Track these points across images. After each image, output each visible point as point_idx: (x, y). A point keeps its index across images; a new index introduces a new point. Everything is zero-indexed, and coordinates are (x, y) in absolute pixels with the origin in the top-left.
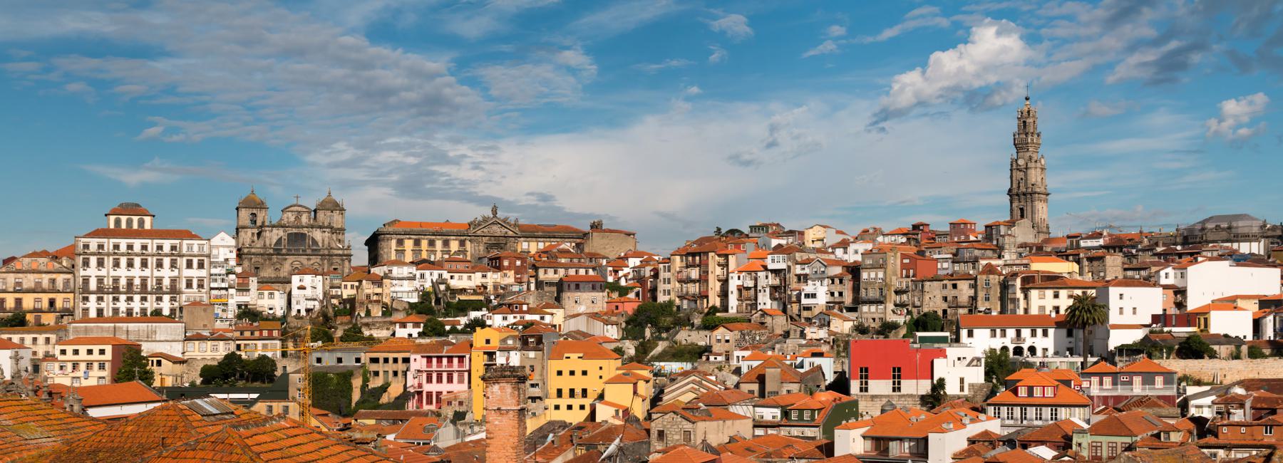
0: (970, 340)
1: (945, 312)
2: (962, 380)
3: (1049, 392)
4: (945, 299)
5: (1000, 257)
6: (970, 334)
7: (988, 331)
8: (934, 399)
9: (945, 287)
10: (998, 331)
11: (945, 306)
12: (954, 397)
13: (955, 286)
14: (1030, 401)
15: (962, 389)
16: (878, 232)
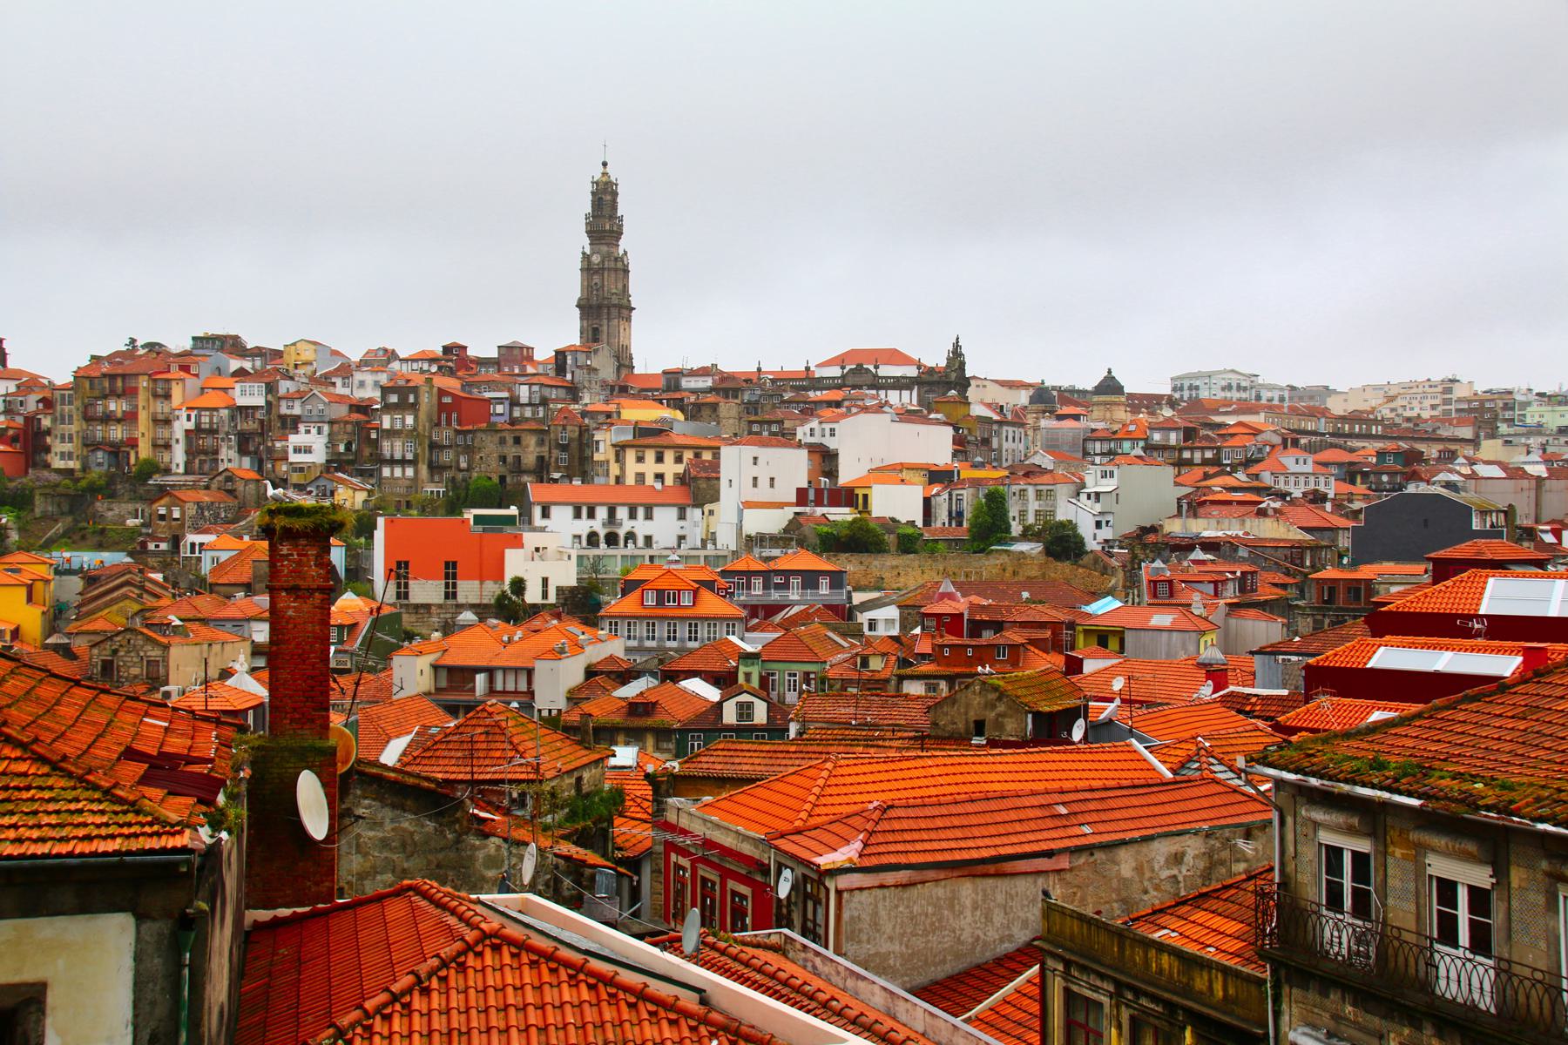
0: (544, 523)
1: (503, 479)
2: (545, 581)
3: (686, 600)
4: (503, 459)
5: (576, 400)
6: (546, 514)
7: (569, 510)
8: (510, 608)
9: (503, 441)
10: (584, 511)
11: (503, 470)
12: (534, 606)
13: (517, 441)
14: (660, 612)
15: (545, 595)
16: (391, 355)
